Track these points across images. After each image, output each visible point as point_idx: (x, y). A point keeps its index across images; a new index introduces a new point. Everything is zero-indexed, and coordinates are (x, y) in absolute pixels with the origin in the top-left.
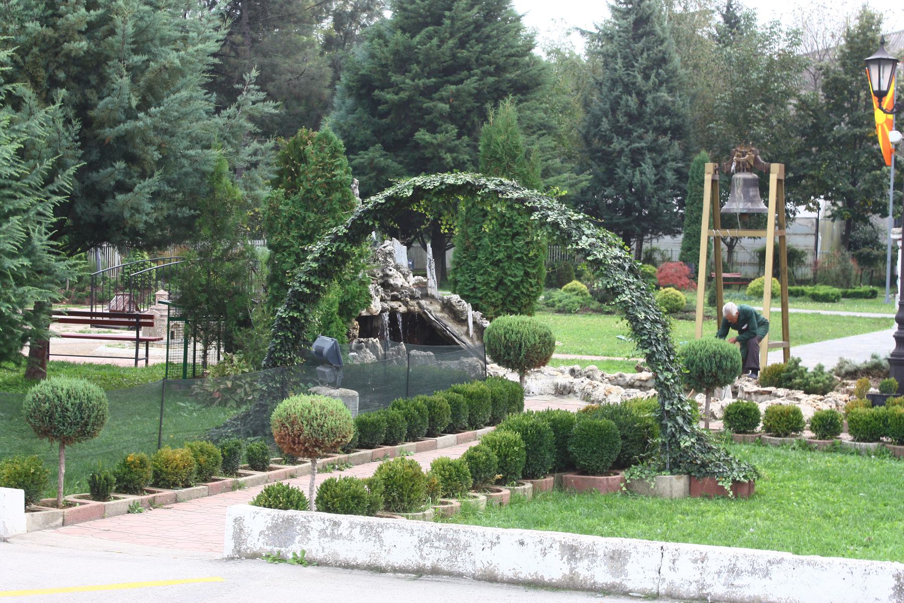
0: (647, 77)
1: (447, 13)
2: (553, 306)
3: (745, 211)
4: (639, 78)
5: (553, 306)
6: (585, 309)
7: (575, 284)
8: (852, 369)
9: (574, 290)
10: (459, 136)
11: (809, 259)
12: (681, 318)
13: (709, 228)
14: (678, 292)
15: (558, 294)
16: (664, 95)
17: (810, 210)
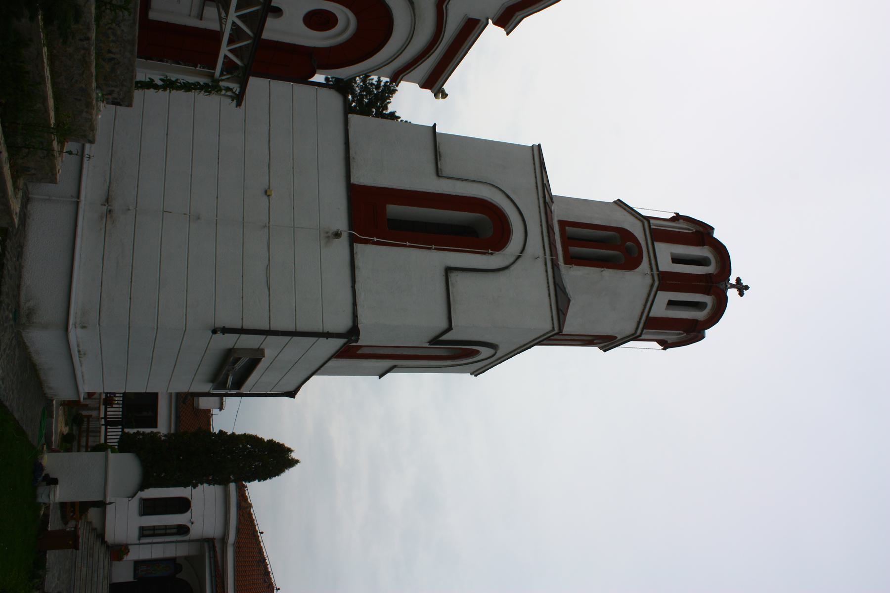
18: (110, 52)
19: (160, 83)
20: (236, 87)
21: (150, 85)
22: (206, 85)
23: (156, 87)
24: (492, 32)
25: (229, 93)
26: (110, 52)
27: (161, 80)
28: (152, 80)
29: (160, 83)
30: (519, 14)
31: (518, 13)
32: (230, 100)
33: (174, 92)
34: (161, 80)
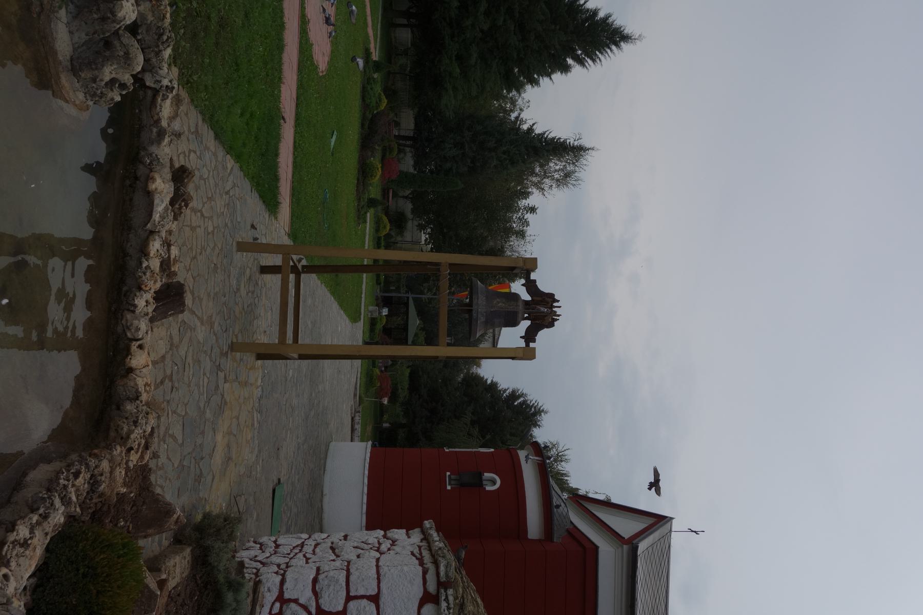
0: (504, 153)
1: (558, 27)
2: (368, 83)
3: (474, 315)
4: (505, 149)
5: (368, 83)
6: (365, 106)
7: (385, 102)
9: (380, 101)
10: (482, 31)
11: (399, 238)
12: (358, 180)
13: (451, 265)
14: (378, 177)
15: (378, 89)
16: (495, 162)
17: (426, 240)
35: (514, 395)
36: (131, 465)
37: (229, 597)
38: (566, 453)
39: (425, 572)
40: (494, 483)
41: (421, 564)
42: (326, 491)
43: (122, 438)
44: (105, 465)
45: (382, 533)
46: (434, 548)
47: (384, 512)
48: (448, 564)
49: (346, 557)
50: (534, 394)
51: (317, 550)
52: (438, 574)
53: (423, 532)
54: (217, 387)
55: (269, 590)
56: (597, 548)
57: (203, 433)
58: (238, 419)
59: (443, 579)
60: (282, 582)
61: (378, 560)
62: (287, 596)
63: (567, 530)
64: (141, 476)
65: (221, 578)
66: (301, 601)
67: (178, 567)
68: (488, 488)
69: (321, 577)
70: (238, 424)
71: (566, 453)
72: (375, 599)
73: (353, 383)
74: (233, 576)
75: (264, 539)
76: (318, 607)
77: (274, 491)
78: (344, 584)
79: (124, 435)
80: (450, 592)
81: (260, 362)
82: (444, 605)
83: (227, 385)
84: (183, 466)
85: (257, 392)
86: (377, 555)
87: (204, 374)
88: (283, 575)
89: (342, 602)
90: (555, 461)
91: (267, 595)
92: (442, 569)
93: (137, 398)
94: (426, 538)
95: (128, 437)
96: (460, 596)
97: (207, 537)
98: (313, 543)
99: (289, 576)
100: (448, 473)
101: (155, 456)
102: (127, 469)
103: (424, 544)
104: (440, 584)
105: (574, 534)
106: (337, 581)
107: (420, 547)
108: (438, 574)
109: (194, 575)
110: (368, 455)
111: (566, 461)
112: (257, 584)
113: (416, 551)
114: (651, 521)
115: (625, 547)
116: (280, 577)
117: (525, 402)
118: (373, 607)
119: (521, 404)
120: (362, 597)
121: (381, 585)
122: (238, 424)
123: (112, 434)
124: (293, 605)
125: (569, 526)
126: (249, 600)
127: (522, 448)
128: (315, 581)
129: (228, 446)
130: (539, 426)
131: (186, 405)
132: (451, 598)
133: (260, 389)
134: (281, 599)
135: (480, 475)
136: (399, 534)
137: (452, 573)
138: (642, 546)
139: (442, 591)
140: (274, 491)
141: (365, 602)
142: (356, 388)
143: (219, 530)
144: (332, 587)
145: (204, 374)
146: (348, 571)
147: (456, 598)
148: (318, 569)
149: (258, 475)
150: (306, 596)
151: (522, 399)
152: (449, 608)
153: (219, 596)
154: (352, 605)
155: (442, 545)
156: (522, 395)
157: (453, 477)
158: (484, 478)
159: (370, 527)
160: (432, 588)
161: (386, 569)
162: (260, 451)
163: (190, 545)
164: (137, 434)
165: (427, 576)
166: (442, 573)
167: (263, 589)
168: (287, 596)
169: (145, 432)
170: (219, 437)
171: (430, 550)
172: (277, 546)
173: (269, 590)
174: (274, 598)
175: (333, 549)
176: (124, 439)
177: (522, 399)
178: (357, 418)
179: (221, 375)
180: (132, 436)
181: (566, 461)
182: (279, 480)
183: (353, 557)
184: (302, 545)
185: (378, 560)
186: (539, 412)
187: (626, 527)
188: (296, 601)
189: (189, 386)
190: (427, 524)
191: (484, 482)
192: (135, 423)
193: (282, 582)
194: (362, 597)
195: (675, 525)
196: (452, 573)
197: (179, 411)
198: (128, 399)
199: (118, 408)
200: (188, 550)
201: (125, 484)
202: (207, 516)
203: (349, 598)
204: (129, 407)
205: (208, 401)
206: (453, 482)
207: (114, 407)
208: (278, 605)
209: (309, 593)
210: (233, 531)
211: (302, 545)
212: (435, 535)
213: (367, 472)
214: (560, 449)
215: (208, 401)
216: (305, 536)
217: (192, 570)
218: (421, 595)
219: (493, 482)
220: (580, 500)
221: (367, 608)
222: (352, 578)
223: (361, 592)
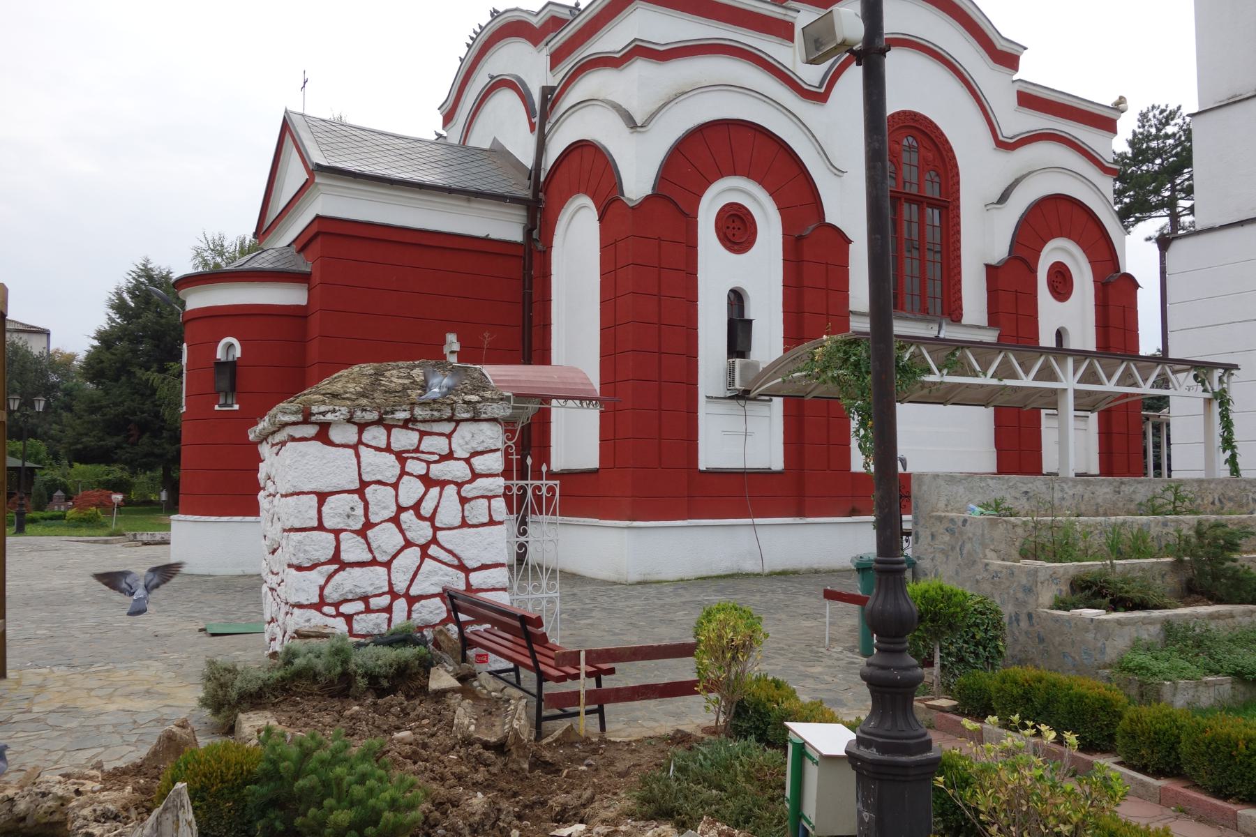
8: (253, 687)
18: (1213, 503)
19: (1228, 453)
20: (1218, 373)
21: (1232, 461)
22: (1221, 405)
23: (1233, 456)
24: (1031, 71)
25: (1225, 379)
26: (1213, 503)
27: (1224, 451)
28: (1227, 461)
29: (1228, 453)
30: (1000, 45)
31: (999, 47)
32: (1233, 378)
33: (1235, 437)
34: (1224, 451)
35: (119, 306)
36: (98, 786)
37: (299, 662)
38: (210, 239)
39: (293, 439)
40: (232, 345)
41: (283, 444)
42: (238, 571)
43: (62, 805)
44: (86, 812)
45: (262, 494)
46: (272, 429)
47: (237, 494)
48: (284, 411)
49: (279, 534)
50: (117, 277)
51: (275, 571)
52: (294, 424)
53: (261, 442)
54: (33, 720)
55: (309, 620)
56: (318, 218)
57: (98, 727)
58: (92, 689)
59: (300, 418)
60: (300, 606)
61: (282, 496)
62: (316, 600)
63: (301, 250)
64: (115, 777)
65: (277, 674)
66: (322, 582)
67: (252, 723)
68: (238, 353)
69: (295, 562)
70: (101, 688)
71: (210, 239)
72: (322, 497)
73: (81, 546)
74: (280, 662)
75: (267, 637)
76: (330, 562)
77: (214, 635)
78: (304, 534)
79: (59, 803)
80: (315, 409)
81: (10, 674)
82: (329, 417)
83: (35, 709)
84: (138, 740)
85: (61, 671)
86: (278, 496)
87: (10, 738)
88: (294, 606)
89: (324, 534)
90: (221, 254)
91: (313, 622)
92: (287, 418)
93: (11, 800)
94: (264, 438)
95: (61, 798)
96: (322, 398)
97: (228, 698)
98: (271, 576)
99: (292, 600)
100: (217, 408)
101: (99, 766)
102: (102, 790)
103: (270, 440)
104: (306, 421)
105: (304, 243)
106: (300, 542)
107: (273, 445)
108: (294, 424)
109: (273, 705)
110: (189, 517)
111: (222, 238)
112: (300, 635)
113: (275, 449)
114: (288, 139)
115: (317, 180)
116: (296, 611)
117: (130, 292)
118: (330, 499)
119: (134, 297)
120: (320, 512)
121: (306, 490)
122: (101, 688)
123: (57, 817)
124: (326, 592)
125: (294, 248)
126: (314, 641)
127: (183, 304)
128: (299, 568)
129: (128, 696)
130: (169, 273)
131: (49, 751)
132: (323, 408)
133: (55, 669)
134: (318, 607)
135: (220, 364)
136: (263, 469)
137: (294, 406)
138: (317, 157)
139: (313, 418)
140: (214, 635)
141: (324, 509)
142: (95, 542)
143: (222, 686)
144: (307, 548)
145: (10, 738)
146: (290, 530)
147: (324, 403)
148: (290, 566)
149: (184, 655)
150: (317, 577)
151: (125, 295)
152: (334, 411)
153: (299, 674)
154: (328, 523)
155: (267, 418)
156: (119, 295)
157: (222, 401)
158: (223, 359)
159: (254, 510)
160: (311, 431)
161: (288, 486)
162: (150, 658)
163: (236, 716)
164: (59, 790)
165: (297, 436)
166: (292, 418)
167: (306, 628)
168: (316, 600)
169: (60, 782)
170: (112, 707)
171: (273, 433)
172: (273, 620)
173: (309, 620)
174: (318, 613)
175: (273, 553)
176: (63, 801)
177: (125, 295)
178: (145, 537)
179: (16, 718)
180: (60, 793)
181: (222, 238)
182: (201, 630)
183: (279, 526)
184: (272, 589)
185: (282, 496)
186: (147, 272)
187: (294, 176)
188: (322, 588)
189: (22, 752)
190: (252, 437)
191: (230, 359)
192: (44, 795)
193: (300, 606)
194: (320, 512)
195: (296, 107)
196: (294, 406)
197: (55, 758)
198: (10, 810)
199: (23, 819)
200: (241, 716)
201: (122, 789)
202: (204, 703)
203: (321, 527)
204: (22, 806)
205: (53, 727)
206: (229, 401)
207: (21, 825)
208: (326, 609)
209: (313, 574)
210: (225, 669)
211: (272, 589)
212: (261, 426)
213: (213, 518)
214: (204, 246)
215: (53, 727)
216: (265, 588)
217: (265, 709)
218: (319, 443)
219: (229, 348)
220: (263, 230)
221: (333, 505)
222: (297, 525)
223: (314, 513)
